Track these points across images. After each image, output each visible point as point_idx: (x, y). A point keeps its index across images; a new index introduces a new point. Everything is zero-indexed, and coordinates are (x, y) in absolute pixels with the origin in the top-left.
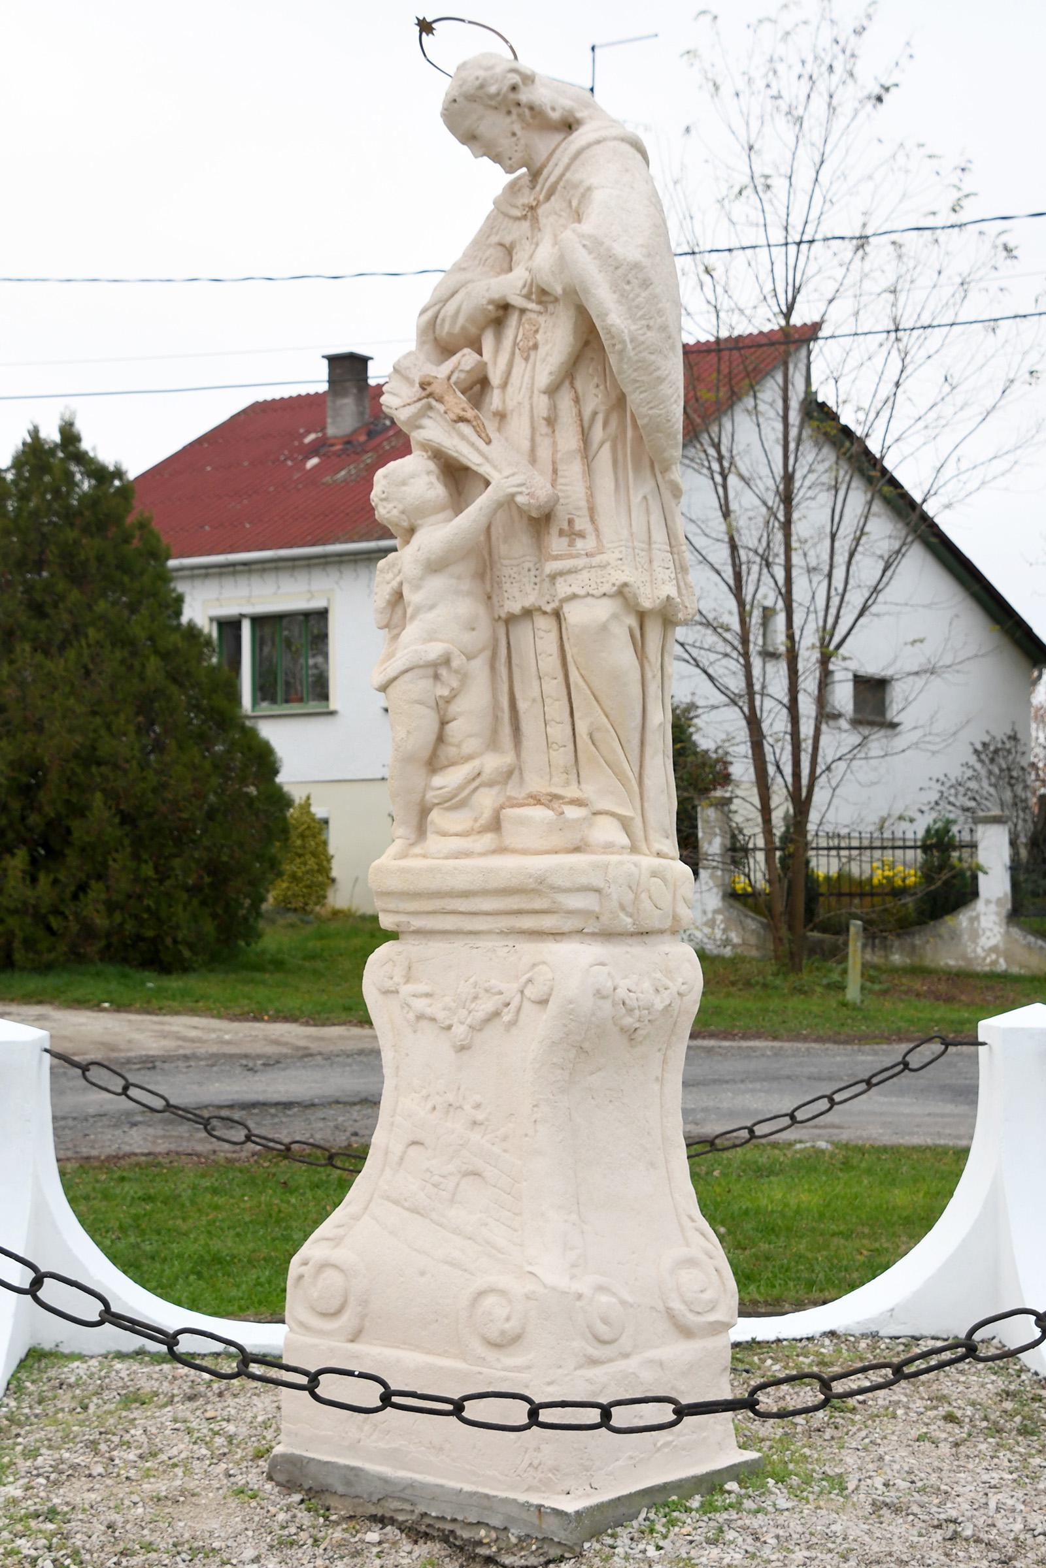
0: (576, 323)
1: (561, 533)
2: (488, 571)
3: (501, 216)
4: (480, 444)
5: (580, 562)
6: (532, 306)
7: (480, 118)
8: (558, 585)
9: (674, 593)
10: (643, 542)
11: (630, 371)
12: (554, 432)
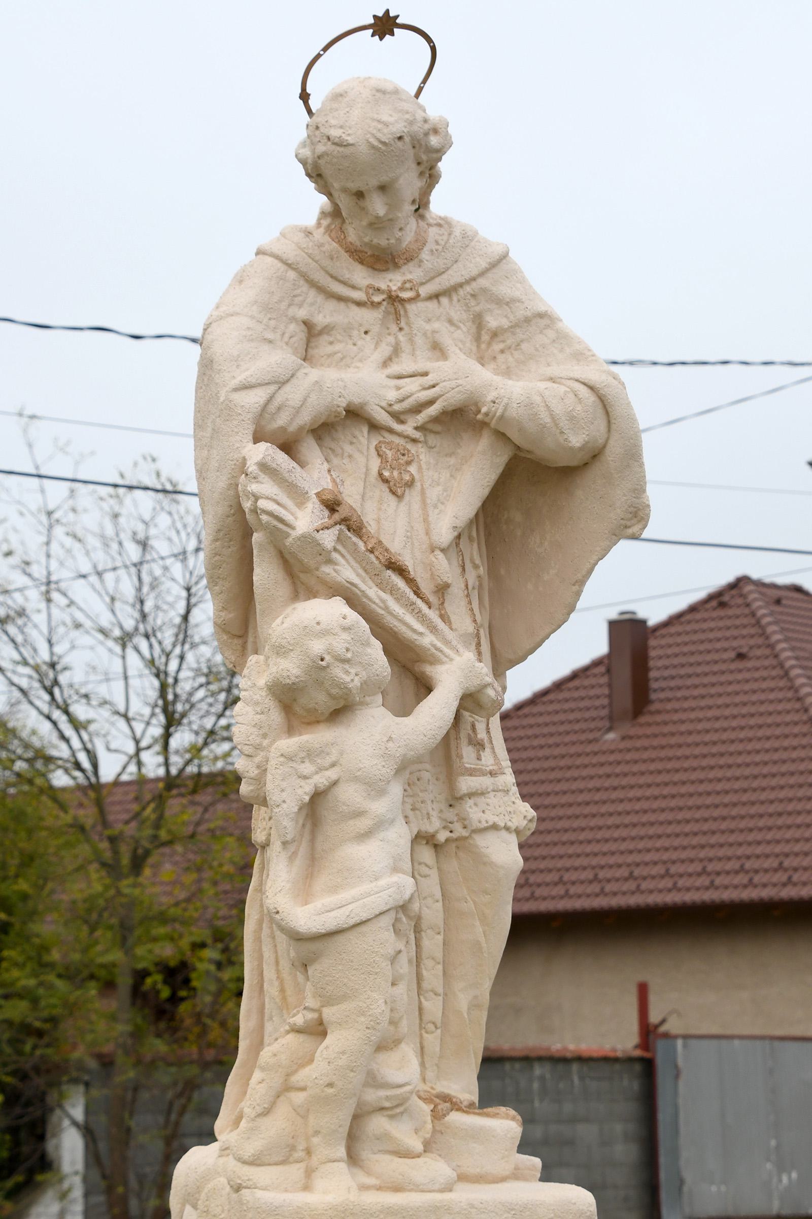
12: (443, 603)
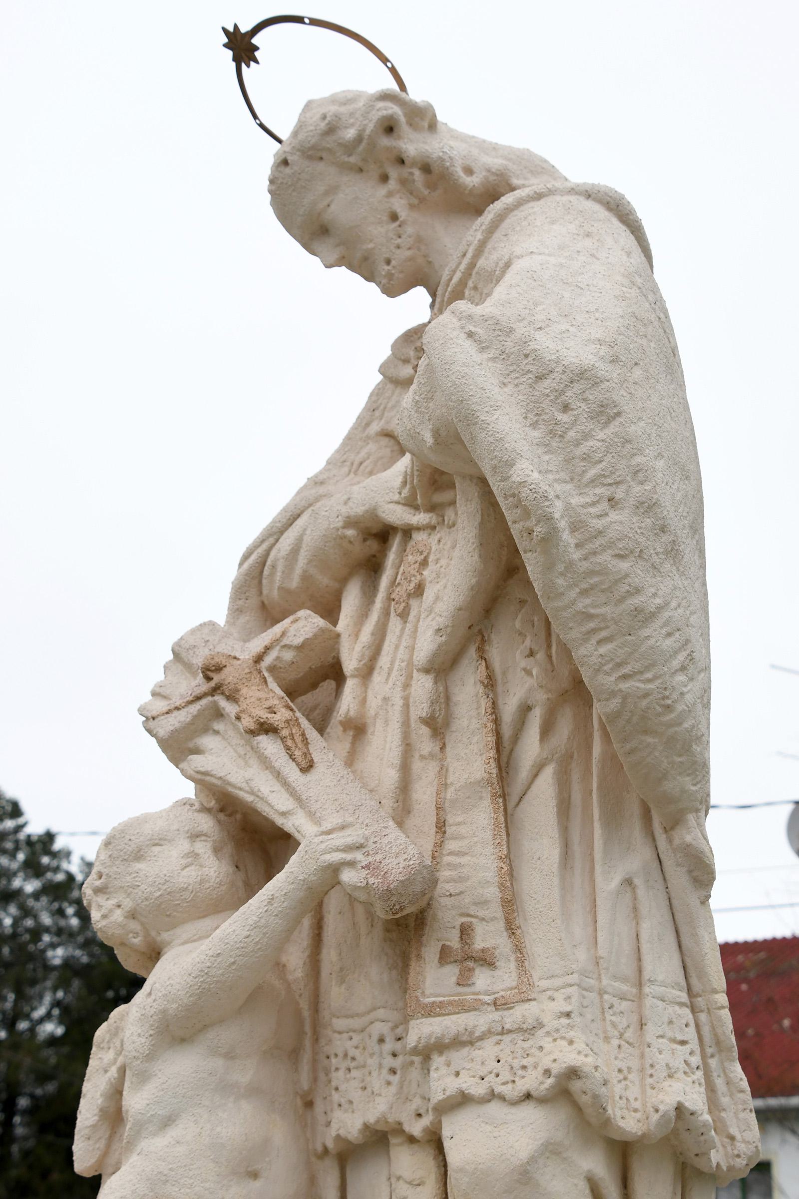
0: (482, 524)
1: (445, 955)
2: (308, 1043)
3: (390, 386)
4: (292, 772)
5: (480, 1021)
6: (421, 518)
7: (332, 190)
8: (433, 1074)
9: (695, 1099)
10: (624, 980)
11: (573, 594)
12: (443, 748)
